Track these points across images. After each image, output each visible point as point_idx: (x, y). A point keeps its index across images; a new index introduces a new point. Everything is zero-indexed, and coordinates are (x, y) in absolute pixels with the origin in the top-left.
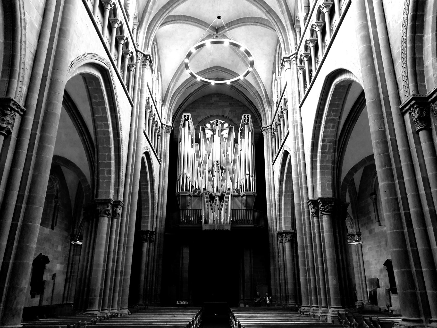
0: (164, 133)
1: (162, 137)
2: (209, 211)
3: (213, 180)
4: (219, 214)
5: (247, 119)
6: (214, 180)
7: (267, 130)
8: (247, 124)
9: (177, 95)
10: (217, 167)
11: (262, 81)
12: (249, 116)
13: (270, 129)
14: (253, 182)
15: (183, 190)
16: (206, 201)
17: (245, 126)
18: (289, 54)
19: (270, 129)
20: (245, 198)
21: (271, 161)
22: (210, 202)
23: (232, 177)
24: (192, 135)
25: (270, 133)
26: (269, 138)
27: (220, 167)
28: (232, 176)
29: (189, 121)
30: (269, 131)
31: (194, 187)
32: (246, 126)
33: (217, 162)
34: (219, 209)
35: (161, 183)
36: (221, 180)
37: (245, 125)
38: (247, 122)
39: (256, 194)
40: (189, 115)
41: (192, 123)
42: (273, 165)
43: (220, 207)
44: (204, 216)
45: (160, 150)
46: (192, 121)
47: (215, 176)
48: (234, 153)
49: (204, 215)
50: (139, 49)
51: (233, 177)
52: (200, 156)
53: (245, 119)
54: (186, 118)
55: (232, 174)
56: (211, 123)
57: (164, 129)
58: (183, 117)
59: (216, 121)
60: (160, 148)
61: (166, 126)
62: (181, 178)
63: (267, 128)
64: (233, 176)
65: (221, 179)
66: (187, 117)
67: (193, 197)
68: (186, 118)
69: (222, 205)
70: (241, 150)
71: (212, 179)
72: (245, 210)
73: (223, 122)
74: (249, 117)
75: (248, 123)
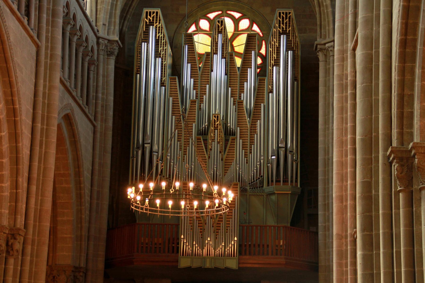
3: (207, 158)
6: (209, 157)
20: (273, 197)
36: (224, 159)
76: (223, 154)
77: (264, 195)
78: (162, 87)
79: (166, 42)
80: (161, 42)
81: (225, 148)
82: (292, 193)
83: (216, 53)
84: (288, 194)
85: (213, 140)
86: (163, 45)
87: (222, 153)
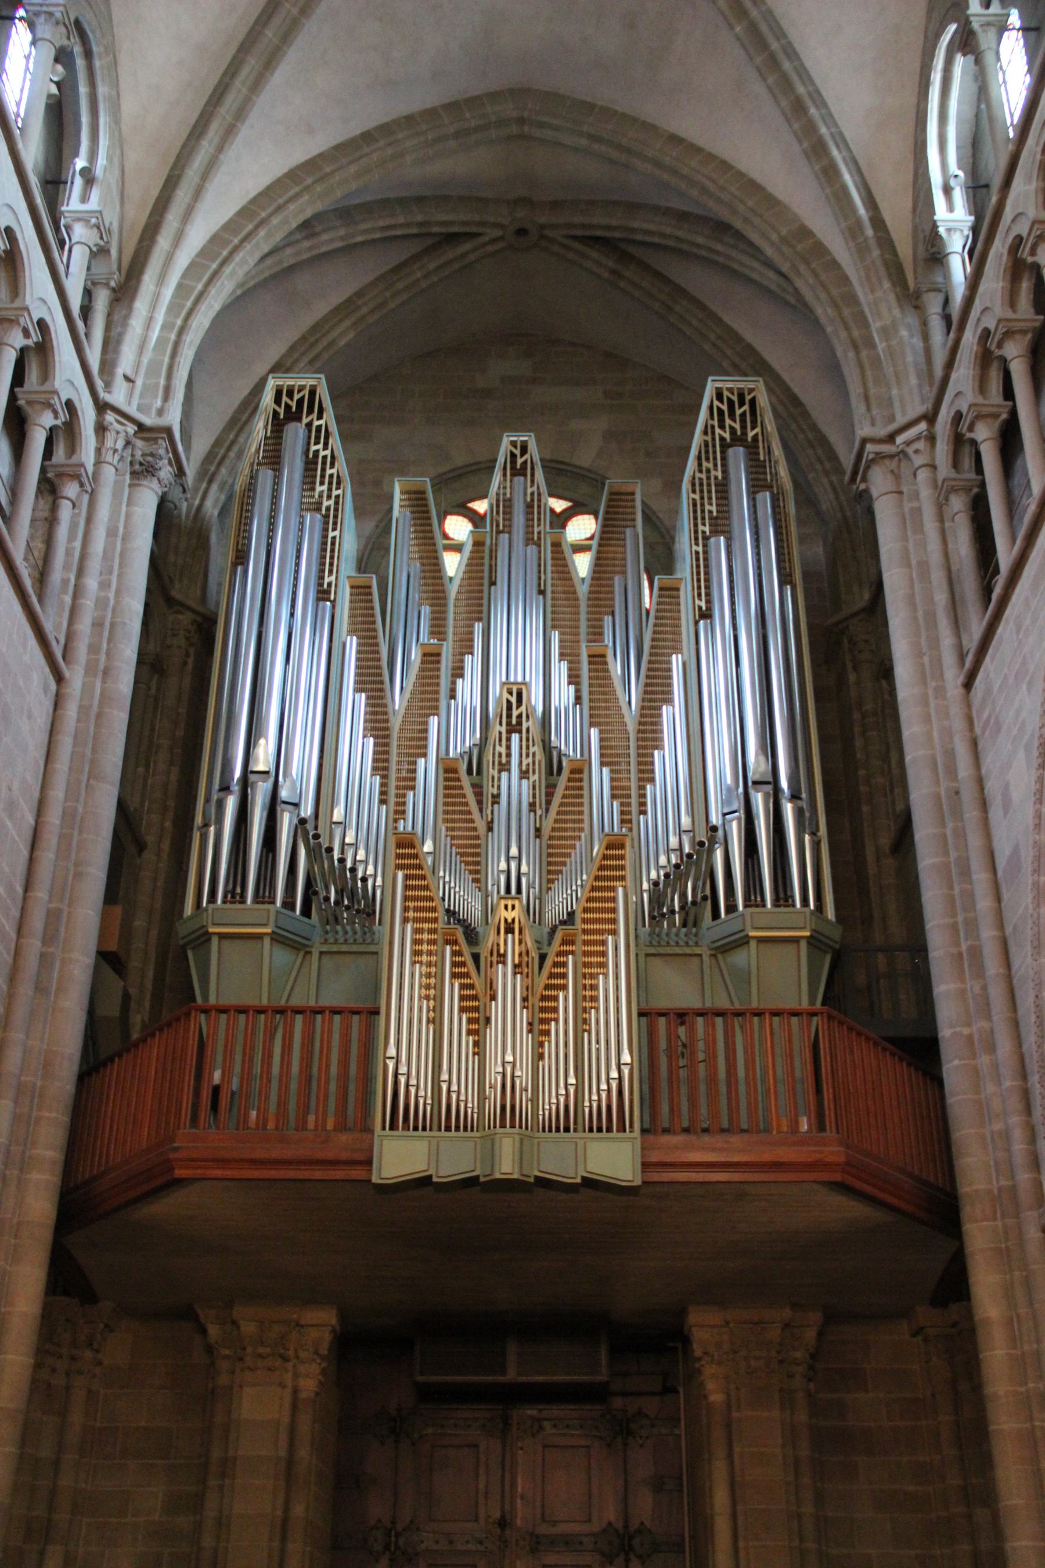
0: (108, 473)
1: (93, 494)
2: (437, 1020)
4: (526, 1042)
5: (738, 412)
6: (490, 829)
7: (902, 455)
8: (738, 439)
9: (231, 254)
10: (515, 737)
11: (841, 135)
12: (751, 391)
13: (921, 445)
14: (807, 837)
15: (236, 894)
16: (416, 942)
17: (724, 459)
18: (892, 419)
19: (921, 445)
21: (949, 658)
22: (447, 942)
23: (634, 808)
24: (330, 520)
25: (923, 475)
26: (919, 510)
27: (538, 738)
28: (634, 801)
29: (309, 425)
30: (918, 460)
31: (330, 850)
32: (738, 456)
33: (514, 700)
34: (525, 999)
35: (54, 817)
36: (546, 832)
37: (725, 446)
38: (743, 427)
39: (836, 934)
40: (313, 392)
41: (335, 441)
42: (968, 684)
43: (540, 990)
44: (391, 1065)
45: (65, 582)
46: (334, 429)
47: (496, 799)
48: (645, 658)
49: (392, 1051)
50: (118, 396)
51: (644, 813)
52: (387, 679)
53: (725, 407)
54: (294, 405)
55: (634, 793)
56: (475, 512)
57: (114, 441)
58: (268, 398)
59: (514, 444)
60: (66, 567)
61: (131, 429)
62: (231, 804)
63: (900, 439)
64: (643, 804)
65: (548, 825)
66: (300, 402)
67: (315, 956)
68: (288, 407)
69: (552, 976)
70: (706, 615)
71: (476, 815)
72: (725, 1124)
73: (559, 505)
74: (753, 402)
75: (751, 434)
76: (541, 816)
77: (700, 955)
78: (321, 603)
79: (338, 477)
80: (323, 476)
81: (548, 803)
82: (811, 937)
83: (508, 529)
84: (796, 940)
85: (505, 767)
86: (330, 483)
87: (539, 812)
